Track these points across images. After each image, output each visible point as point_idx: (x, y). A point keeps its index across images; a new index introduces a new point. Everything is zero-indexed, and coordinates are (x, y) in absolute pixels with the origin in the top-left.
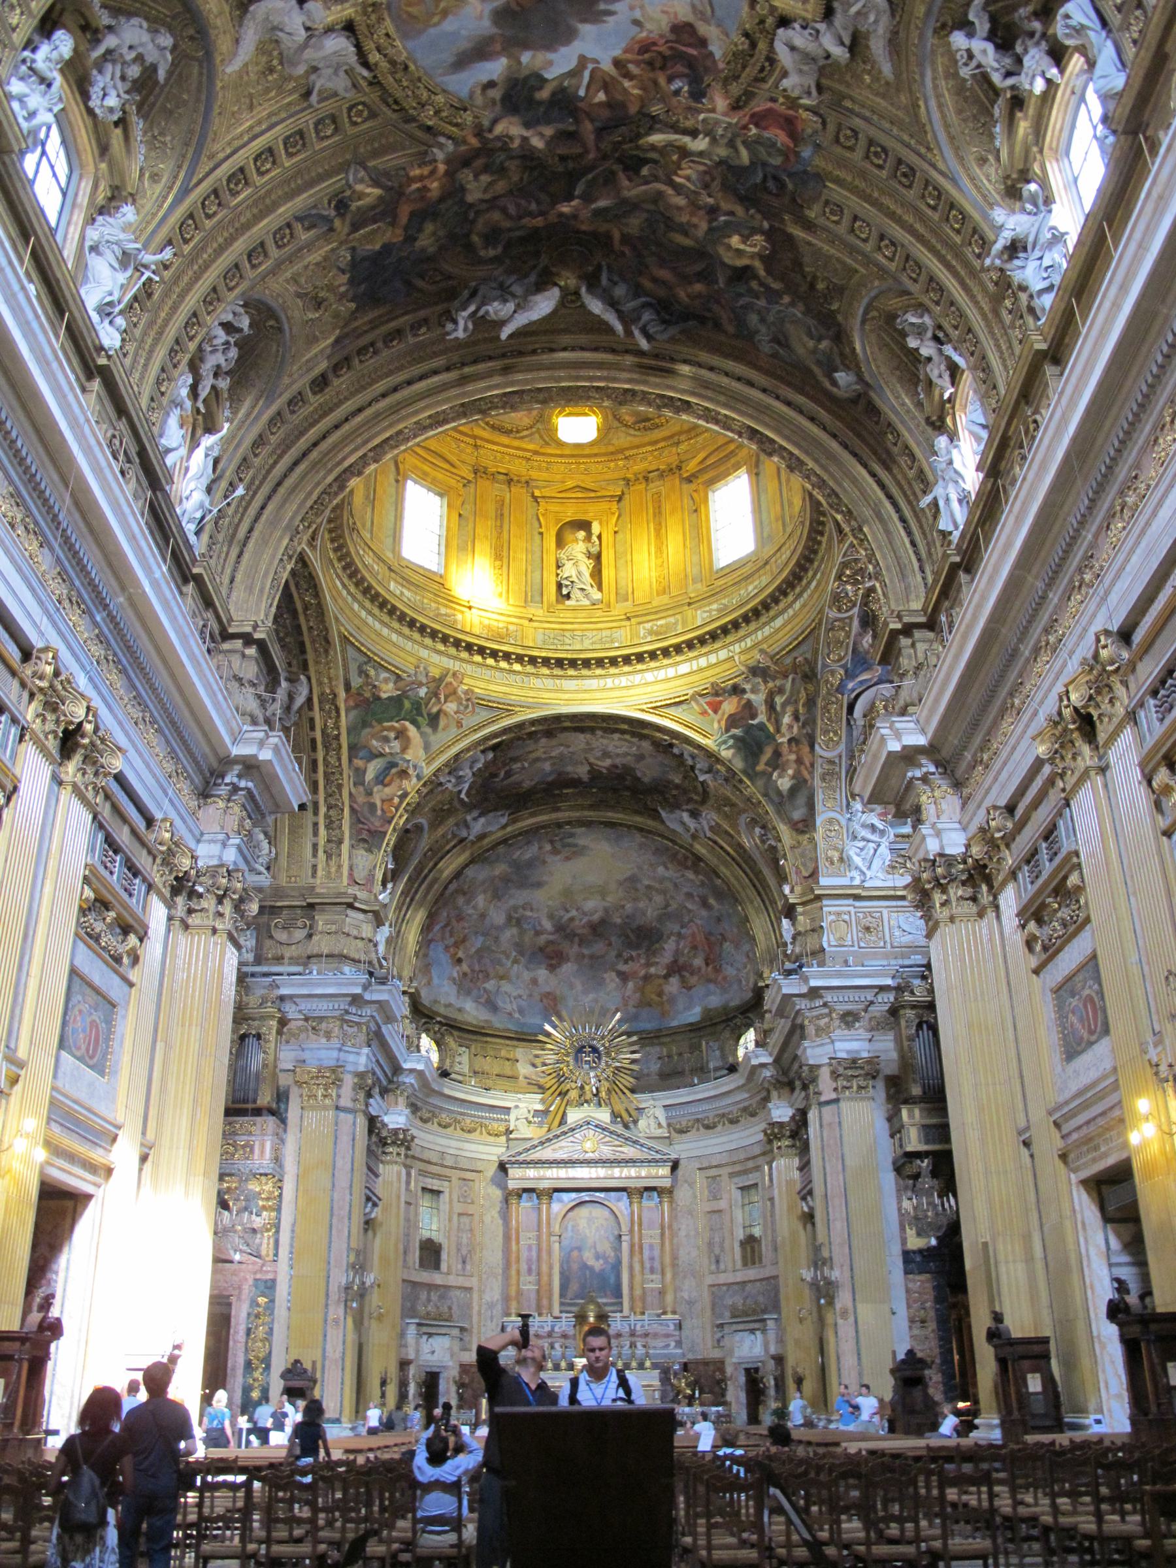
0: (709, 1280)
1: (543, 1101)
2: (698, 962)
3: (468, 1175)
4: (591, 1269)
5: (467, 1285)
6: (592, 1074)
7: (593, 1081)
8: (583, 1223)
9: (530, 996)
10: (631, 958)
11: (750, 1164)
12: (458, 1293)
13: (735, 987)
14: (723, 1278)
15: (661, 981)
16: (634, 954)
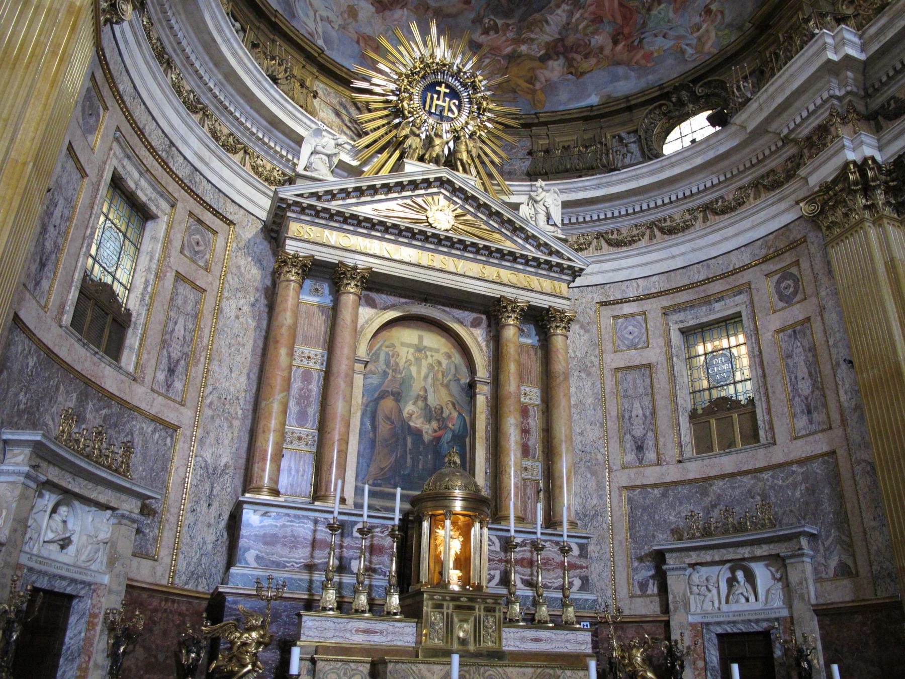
0: (624, 478)
1: (356, 152)
2: (600, 39)
3: (208, 218)
4: (417, 434)
5: (171, 417)
6: (446, 126)
7: (447, 137)
8: (405, 354)
9: (343, 27)
10: (496, 28)
11: (717, 287)
12: (148, 428)
13: (670, 61)
14: (652, 475)
15: (536, 64)
16: (500, 22)
